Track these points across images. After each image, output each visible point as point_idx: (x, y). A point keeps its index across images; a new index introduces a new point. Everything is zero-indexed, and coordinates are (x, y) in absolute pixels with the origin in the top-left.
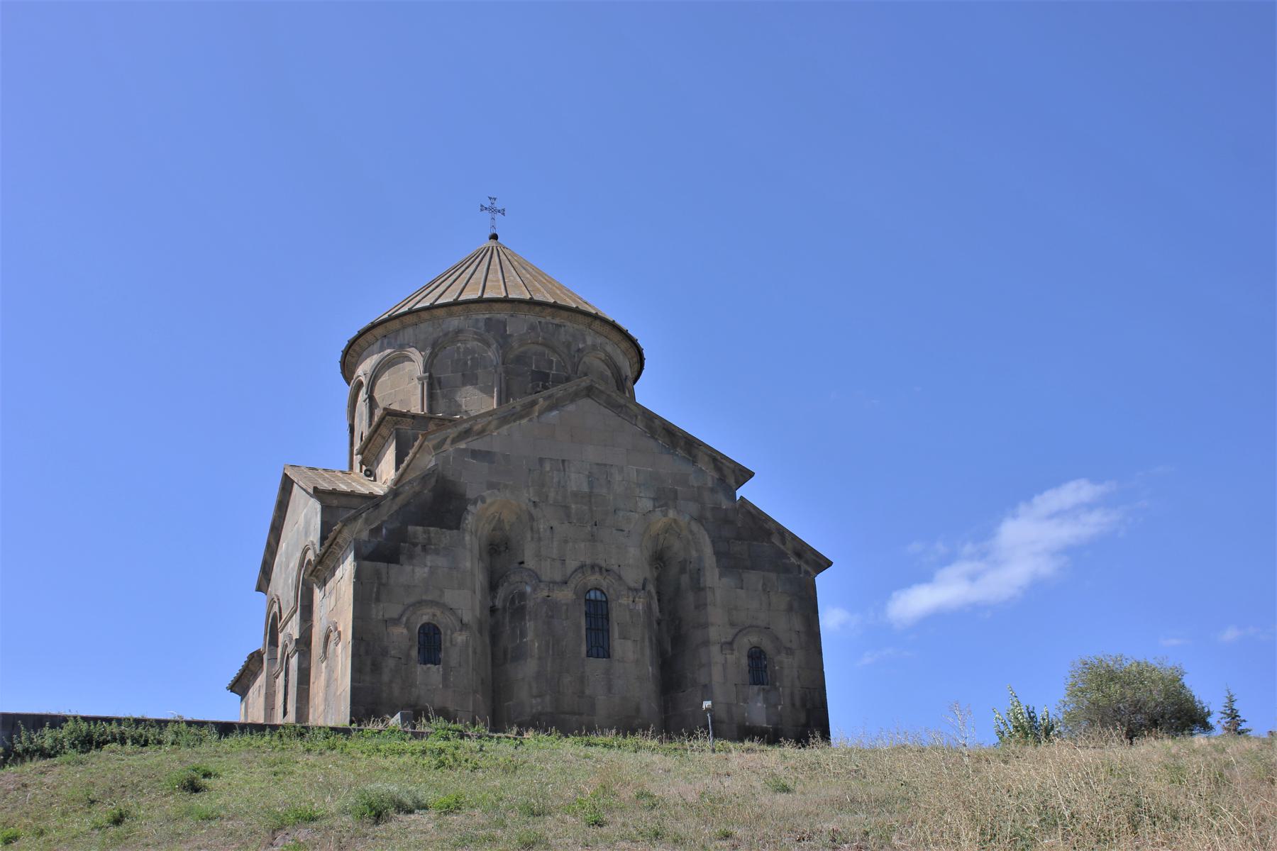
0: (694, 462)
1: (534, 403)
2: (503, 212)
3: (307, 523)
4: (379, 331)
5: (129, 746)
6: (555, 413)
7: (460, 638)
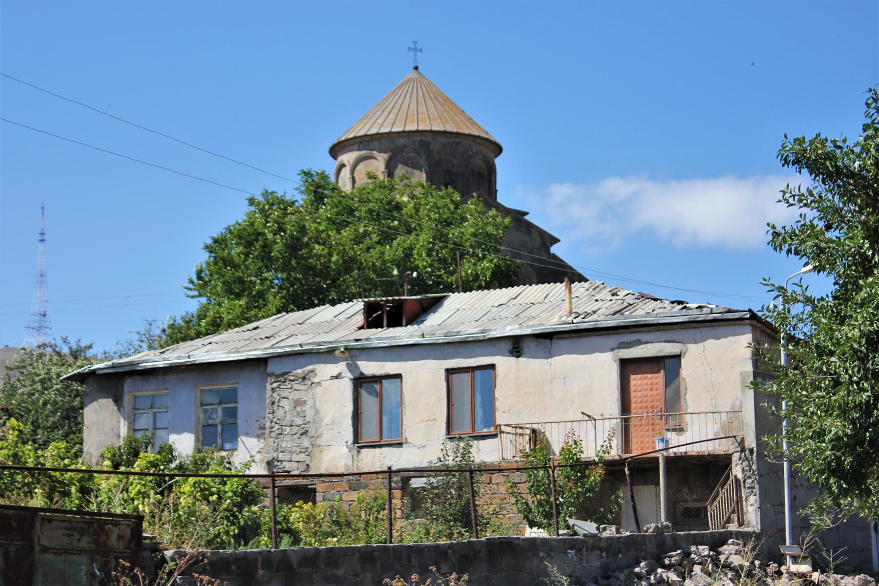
0: (530, 234)
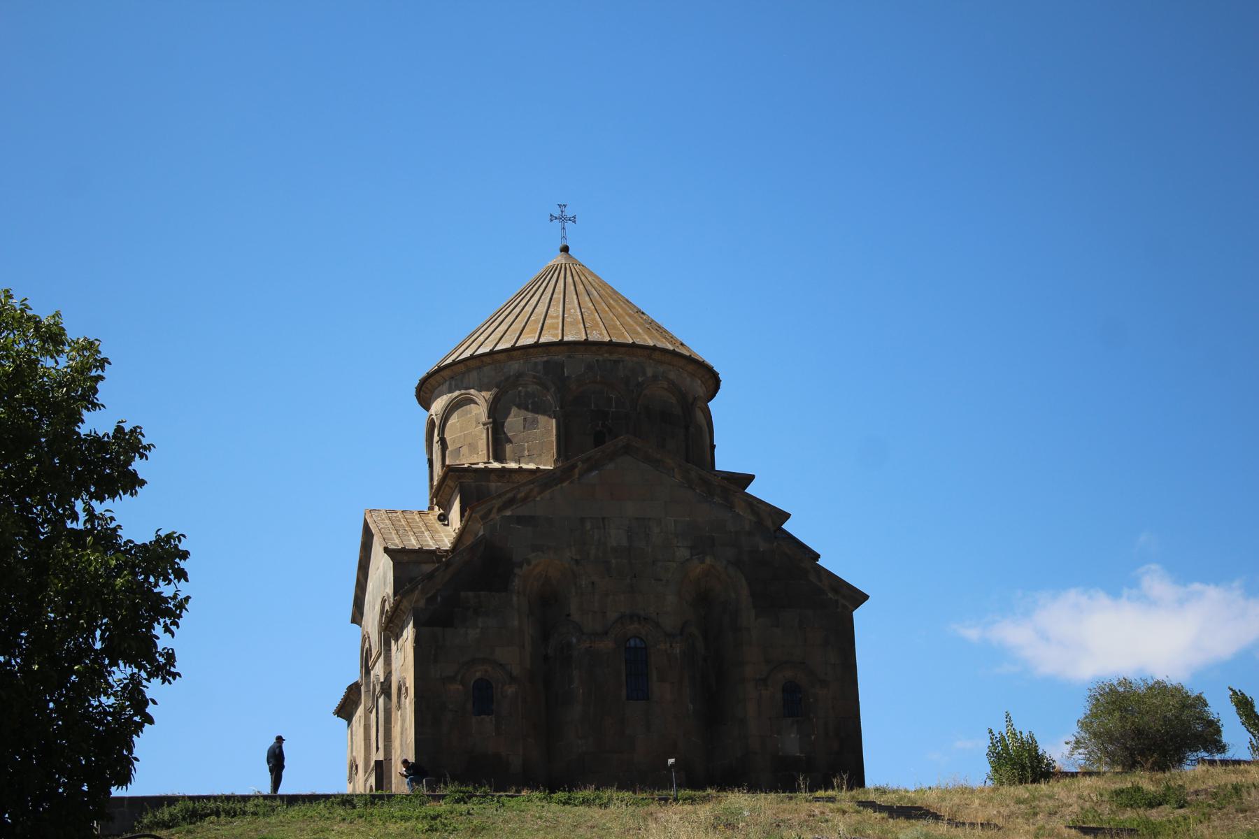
1: (573, 467)
3: (385, 574)
4: (446, 373)
5: (223, 818)
6: (595, 473)
7: (510, 690)
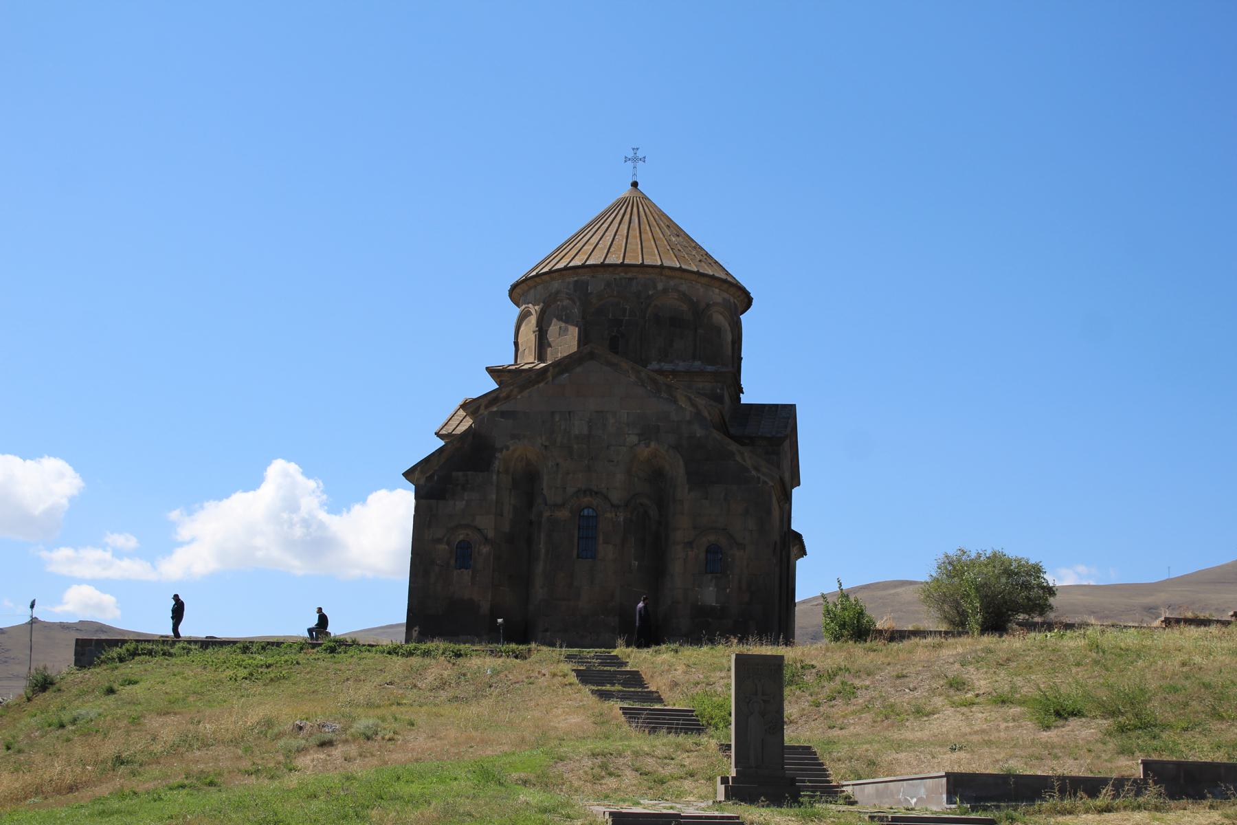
0: (675, 401)
2: (644, 159)
4: (518, 290)
6: (566, 375)
7: (485, 549)
